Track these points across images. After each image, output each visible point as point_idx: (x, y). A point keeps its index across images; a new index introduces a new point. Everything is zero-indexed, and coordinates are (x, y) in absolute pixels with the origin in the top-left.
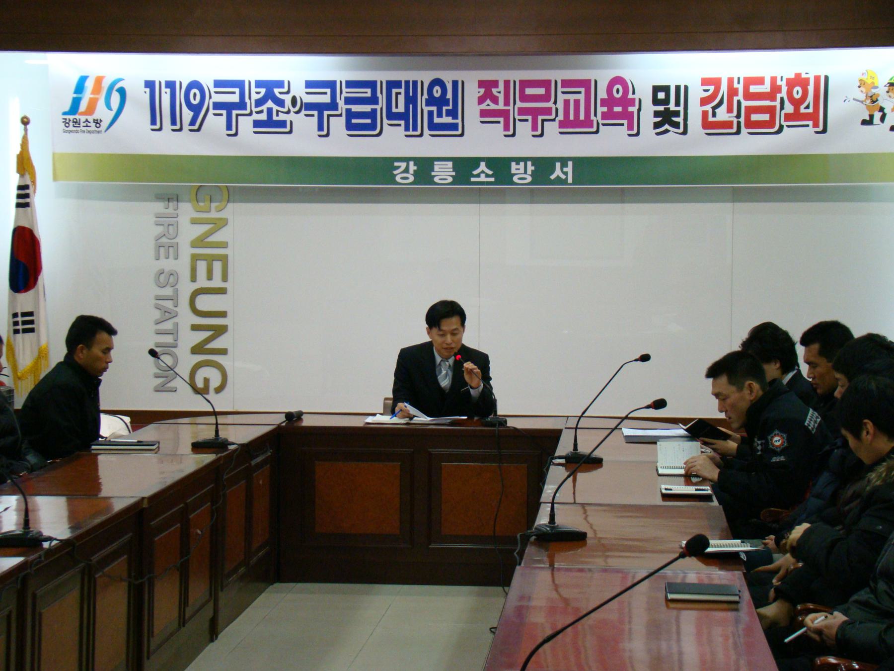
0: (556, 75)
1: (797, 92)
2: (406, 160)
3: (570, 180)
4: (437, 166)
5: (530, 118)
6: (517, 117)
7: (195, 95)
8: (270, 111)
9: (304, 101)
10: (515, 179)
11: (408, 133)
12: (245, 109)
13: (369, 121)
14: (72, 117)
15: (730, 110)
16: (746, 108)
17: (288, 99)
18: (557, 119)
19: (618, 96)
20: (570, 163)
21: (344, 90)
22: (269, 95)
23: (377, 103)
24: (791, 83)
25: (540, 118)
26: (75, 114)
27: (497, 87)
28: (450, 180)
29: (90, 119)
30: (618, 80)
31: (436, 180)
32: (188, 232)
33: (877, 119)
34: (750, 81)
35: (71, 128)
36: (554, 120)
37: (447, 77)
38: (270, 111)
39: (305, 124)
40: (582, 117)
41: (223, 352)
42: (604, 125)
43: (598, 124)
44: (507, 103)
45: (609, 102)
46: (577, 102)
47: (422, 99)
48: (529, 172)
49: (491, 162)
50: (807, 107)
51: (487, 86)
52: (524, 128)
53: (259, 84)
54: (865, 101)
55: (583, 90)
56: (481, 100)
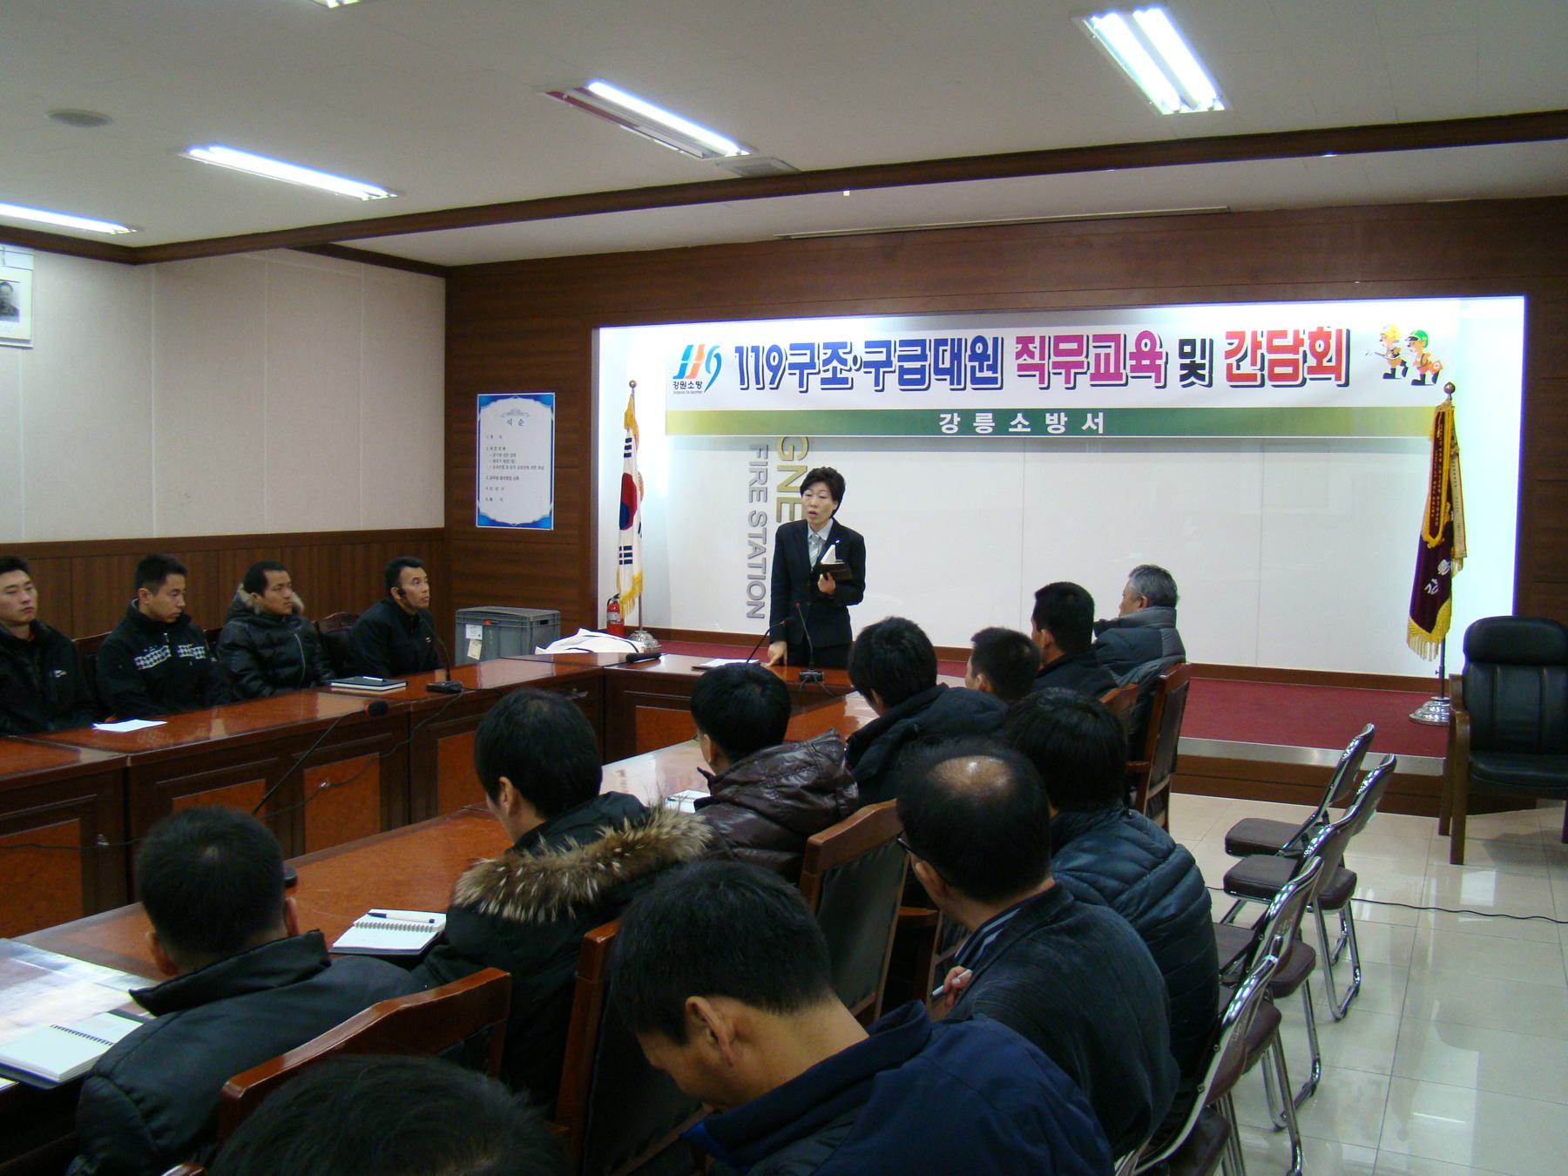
0: (1087, 331)
1: (1320, 346)
2: (951, 412)
3: (1101, 431)
4: (978, 418)
5: (1063, 371)
6: (1052, 371)
7: (774, 357)
8: (835, 369)
13: (919, 376)
14: (679, 380)
15: (1254, 363)
16: (1270, 361)
17: (850, 358)
19: (1146, 350)
20: (1101, 414)
21: (898, 348)
22: (835, 356)
24: (1314, 337)
25: (1073, 371)
26: (682, 378)
27: (1033, 343)
28: (990, 430)
29: (694, 381)
31: (978, 430)
34: (1273, 335)
35: (679, 390)
36: (1085, 373)
37: (988, 334)
38: (835, 369)
39: (864, 380)
40: (1112, 370)
42: (1132, 377)
43: (1127, 376)
44: (1042, 358)
46: (1107, 356)
47: (965, 356)
48: (1063, 423)
49: (1027, 413)
50: (1330, 361)
51: (1025, 341)
52: (1058, 381)
53: (826, 346)
54: (1386, 355)
55: (1113, 344)
56: (1019, 355)
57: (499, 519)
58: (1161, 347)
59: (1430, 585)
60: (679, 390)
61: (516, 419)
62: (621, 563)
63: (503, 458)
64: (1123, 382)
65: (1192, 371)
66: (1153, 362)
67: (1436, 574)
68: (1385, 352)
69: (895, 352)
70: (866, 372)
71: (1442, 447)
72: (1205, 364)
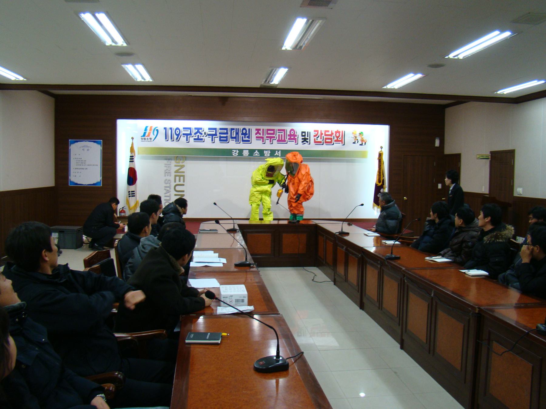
1: (338, 135)
2: (236, 149)
3: (280, 156)
4: (244, 151)
5: (269, 139)
7: (178, 131)
8: (198, 136)
9: (208, 133)
10: (265, 155)
11: (236, 142)
12: (191, 135)
13: (225, 139)
14: (143, 137)
15: (321, 139)
18: (277, 139)
20: (280, 151)
21: (219, 130)
23: (228, 134)
24: (336, 132)
26: (144, 136)
28: (248, 155)
30: (292, 130)
32: (174, 169)
34: (326, 131)
35: (143, 140)
37: (247, 127)
38: (198, 136)
39: (208, 139)
40: (283, 139)
44: (263, 135)
45: (290, 135)
46: (282, 135)
47: (240, 134)
49: (259, 150)
51: (258, 130)
52: (268, 142)
53: (195, 129)
55: (283, 132)
56: (256, 134)
57: (79, 183)
58: (296, 133)
59: (378, 195)
60: (143, 140)
61: (86, 149)
62: (130, 196)
63: (80, 162)
64: (286, 142)
65: (305, 140)
67: (380, 192)
69: (218, 131)
71: (381, 161)
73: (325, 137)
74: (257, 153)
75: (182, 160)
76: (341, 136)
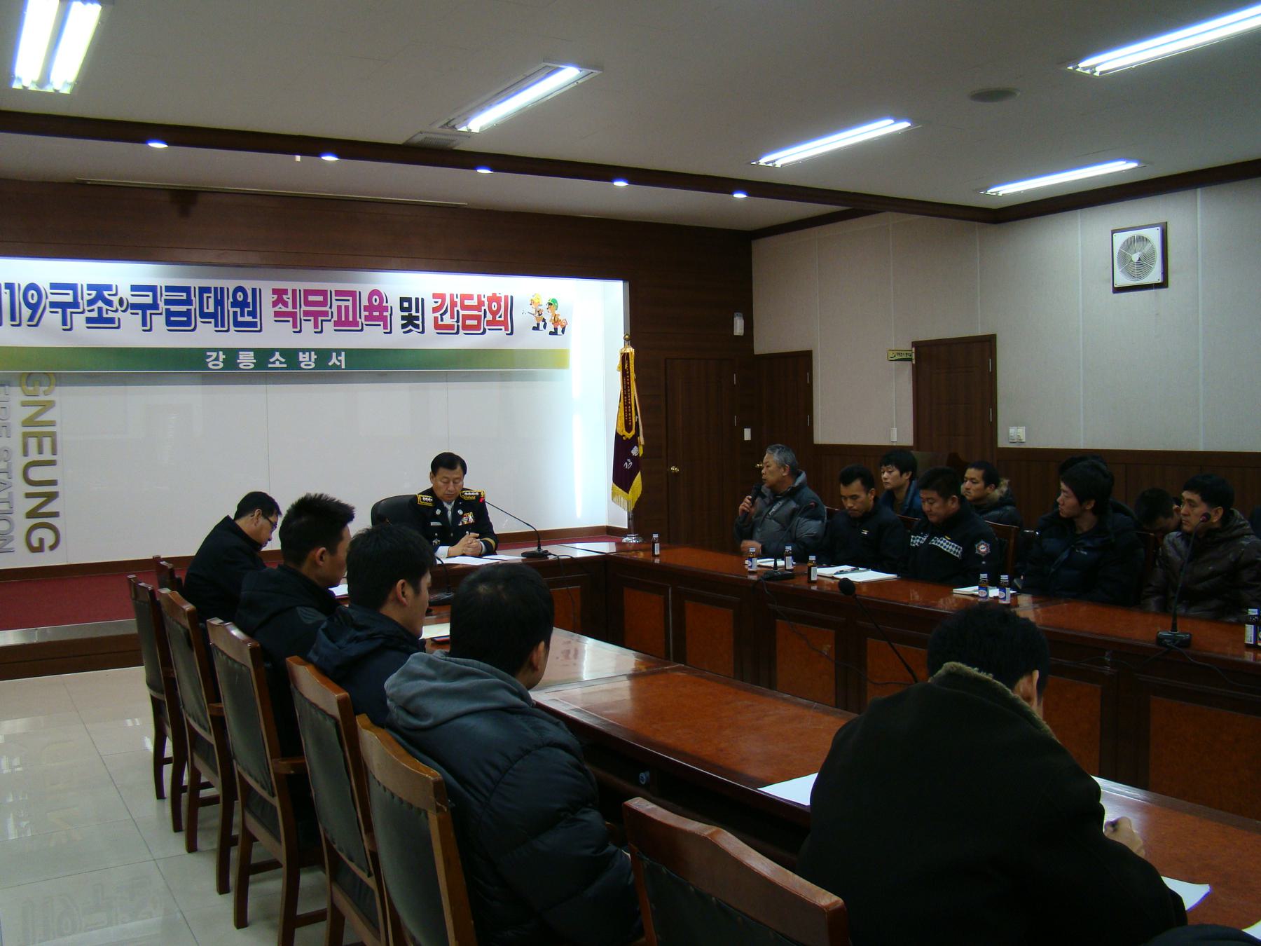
1: (494, 306)
2: (217, 350)
3: (343, 366)
4: (242, 355)
5: (312, 318)
6: (303, 318)
7: (33, 295)
8: (100, 309)
10: (302, 365)
11: (217, 329)
12: (78, 308)
13: (185, 319)
15: (452, 317)
18: (332, 320)
20: (343, 353)
21: (164, 293)
22: (100, 297)
23: (191, 305)
24: (491, 300)
25: (320, 319)
27: (287, 294)
28: (252, 366)
31: (241, 366)
33: (541, 327)
34: (465, 297)
36: (330, 321)
37: (248, 285)
38: (100, 309)
39: (131, 321)
40: (351, 319)
41: (55, 515)
42: (367, 325)
43: (362, 324)
44: (294, 306)
45: (370, 308)
46: (347, 307)
47: (228, 302)
48: (313, 360)
49: (284, 352)
50: (500, 317)
51: (279, 293)
52: (308, 326)
53: (90, 287)
55: (351, 298)
56: (275, 304)
58: (387, 302)
65: (410, 322)
66: (381, 313)
68: (534, 312)
70: (132, 313)
72: (418, 316)
73: (462, 312)
74: (277, 361)
75: (44, 386)
76: (502, 311)
